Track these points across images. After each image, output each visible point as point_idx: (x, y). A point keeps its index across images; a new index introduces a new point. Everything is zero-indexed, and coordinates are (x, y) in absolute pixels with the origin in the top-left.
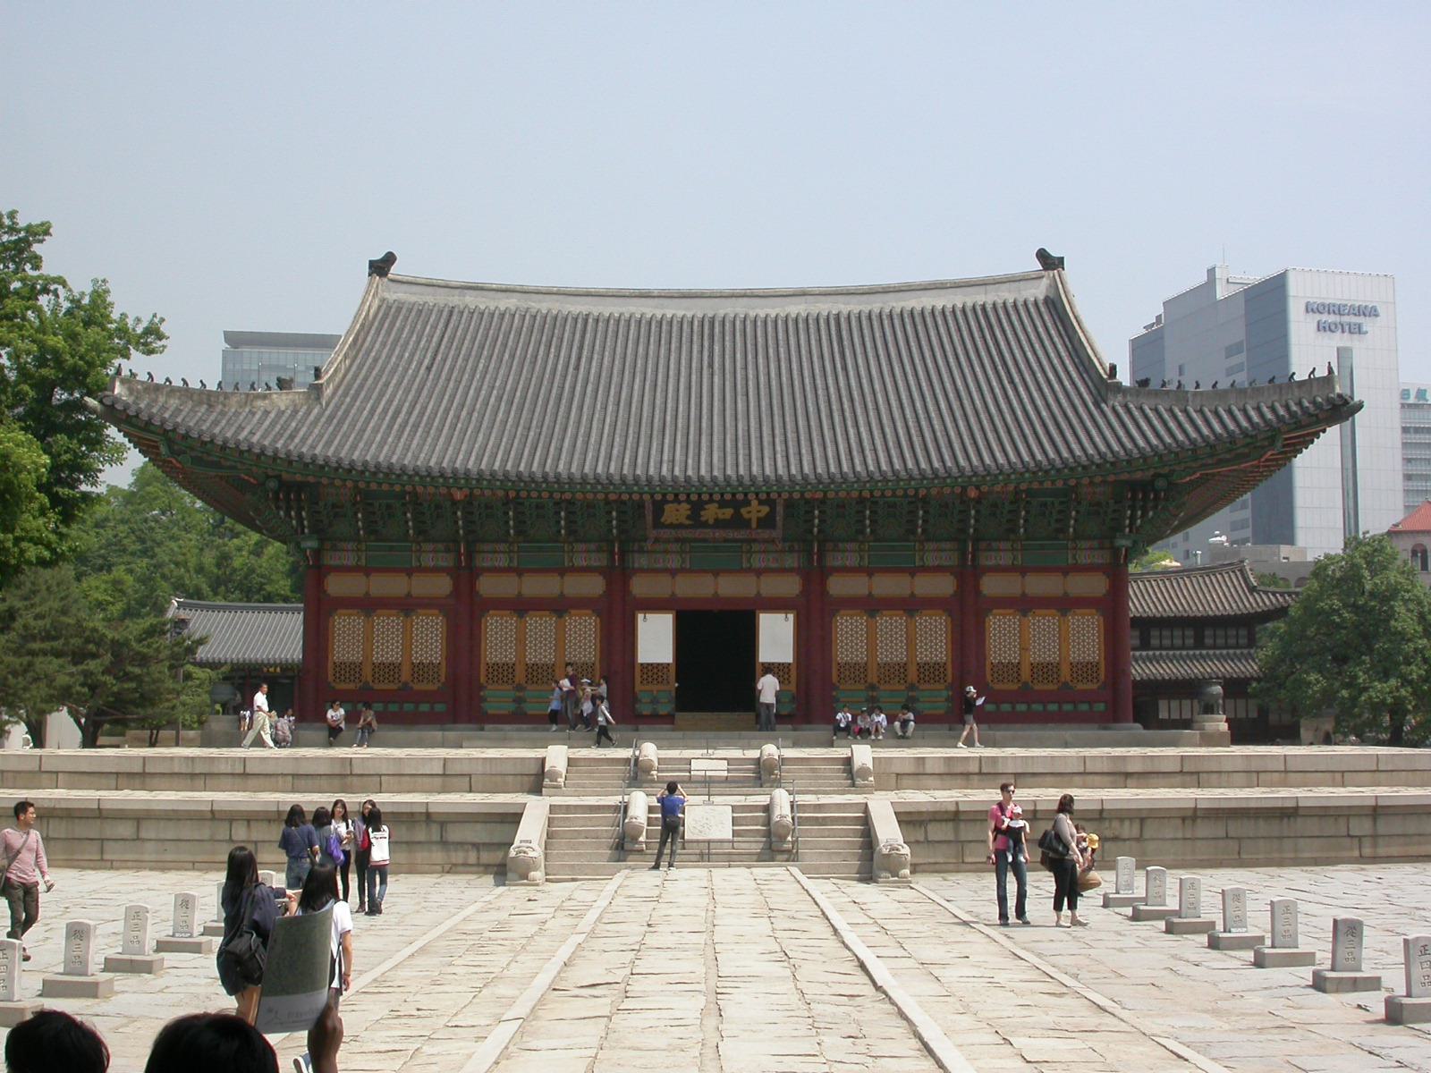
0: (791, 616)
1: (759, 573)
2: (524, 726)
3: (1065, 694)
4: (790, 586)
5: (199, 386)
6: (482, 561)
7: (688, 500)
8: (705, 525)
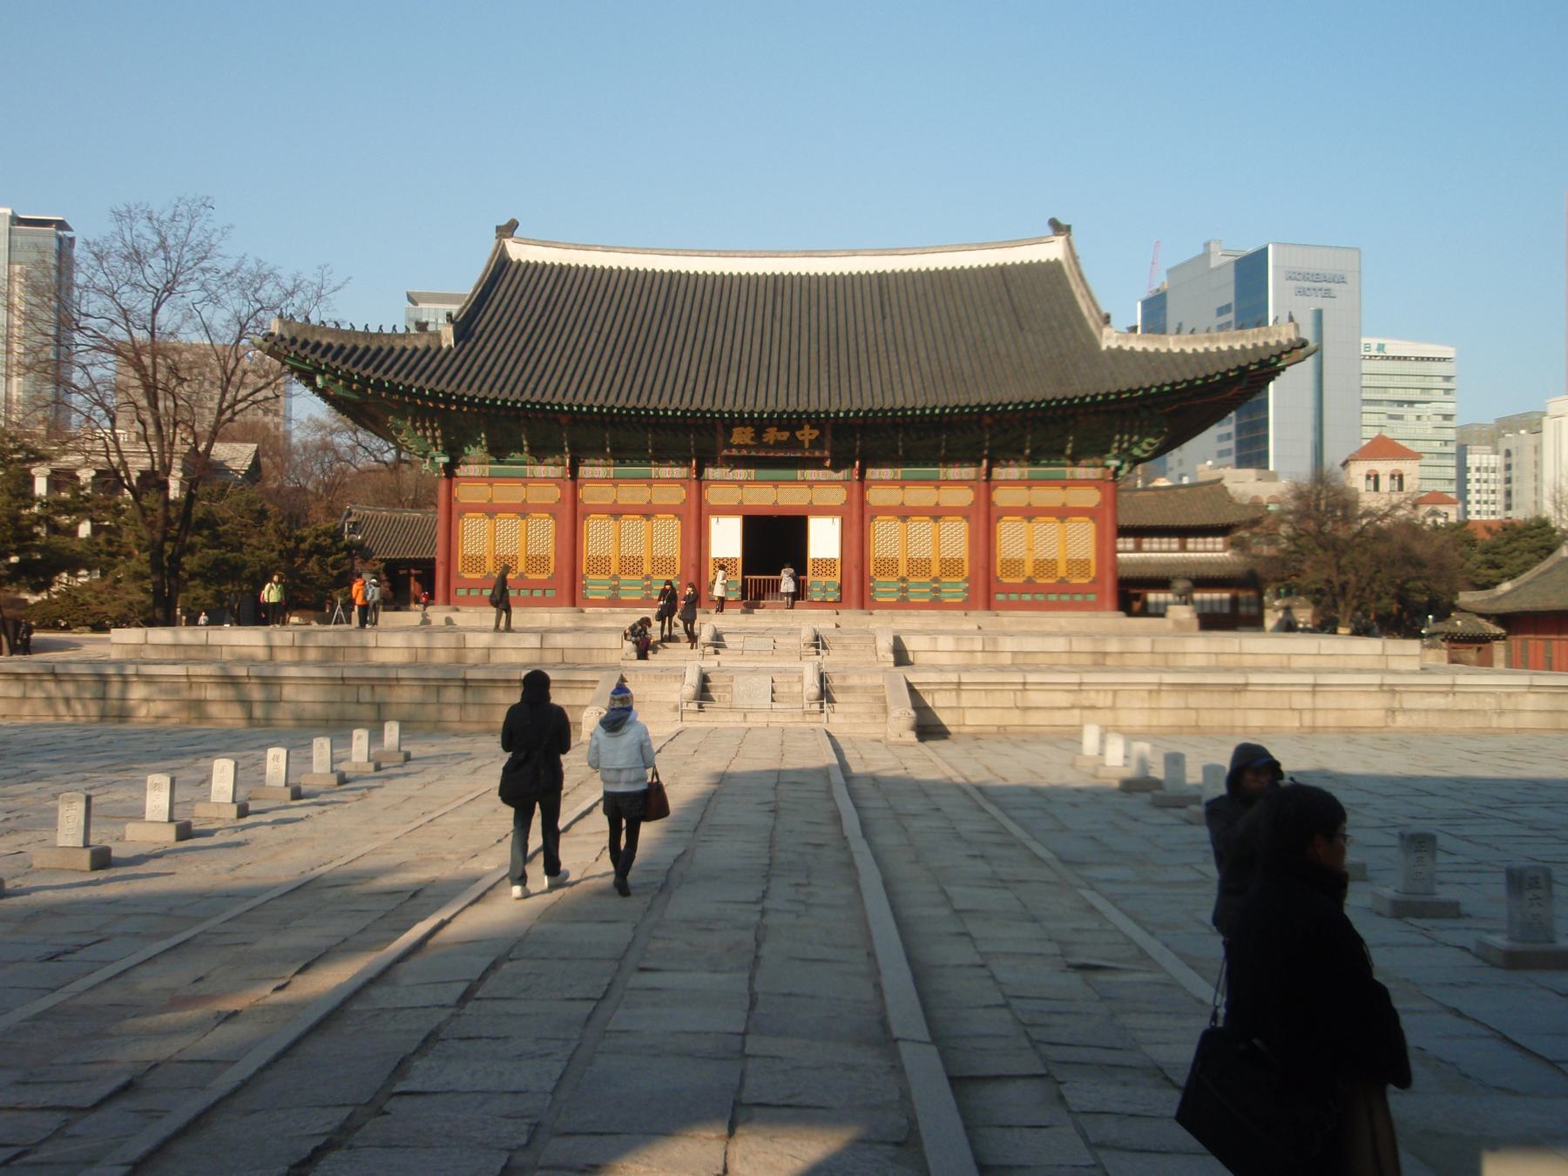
0: (837, 521)
1: (811, 484)
2: (618, 609)
3: (1063, 586)
4: (836, 496)
5: (348, 327)
6: (585, 471)
7: (752, 425)
8: (767, 446)
